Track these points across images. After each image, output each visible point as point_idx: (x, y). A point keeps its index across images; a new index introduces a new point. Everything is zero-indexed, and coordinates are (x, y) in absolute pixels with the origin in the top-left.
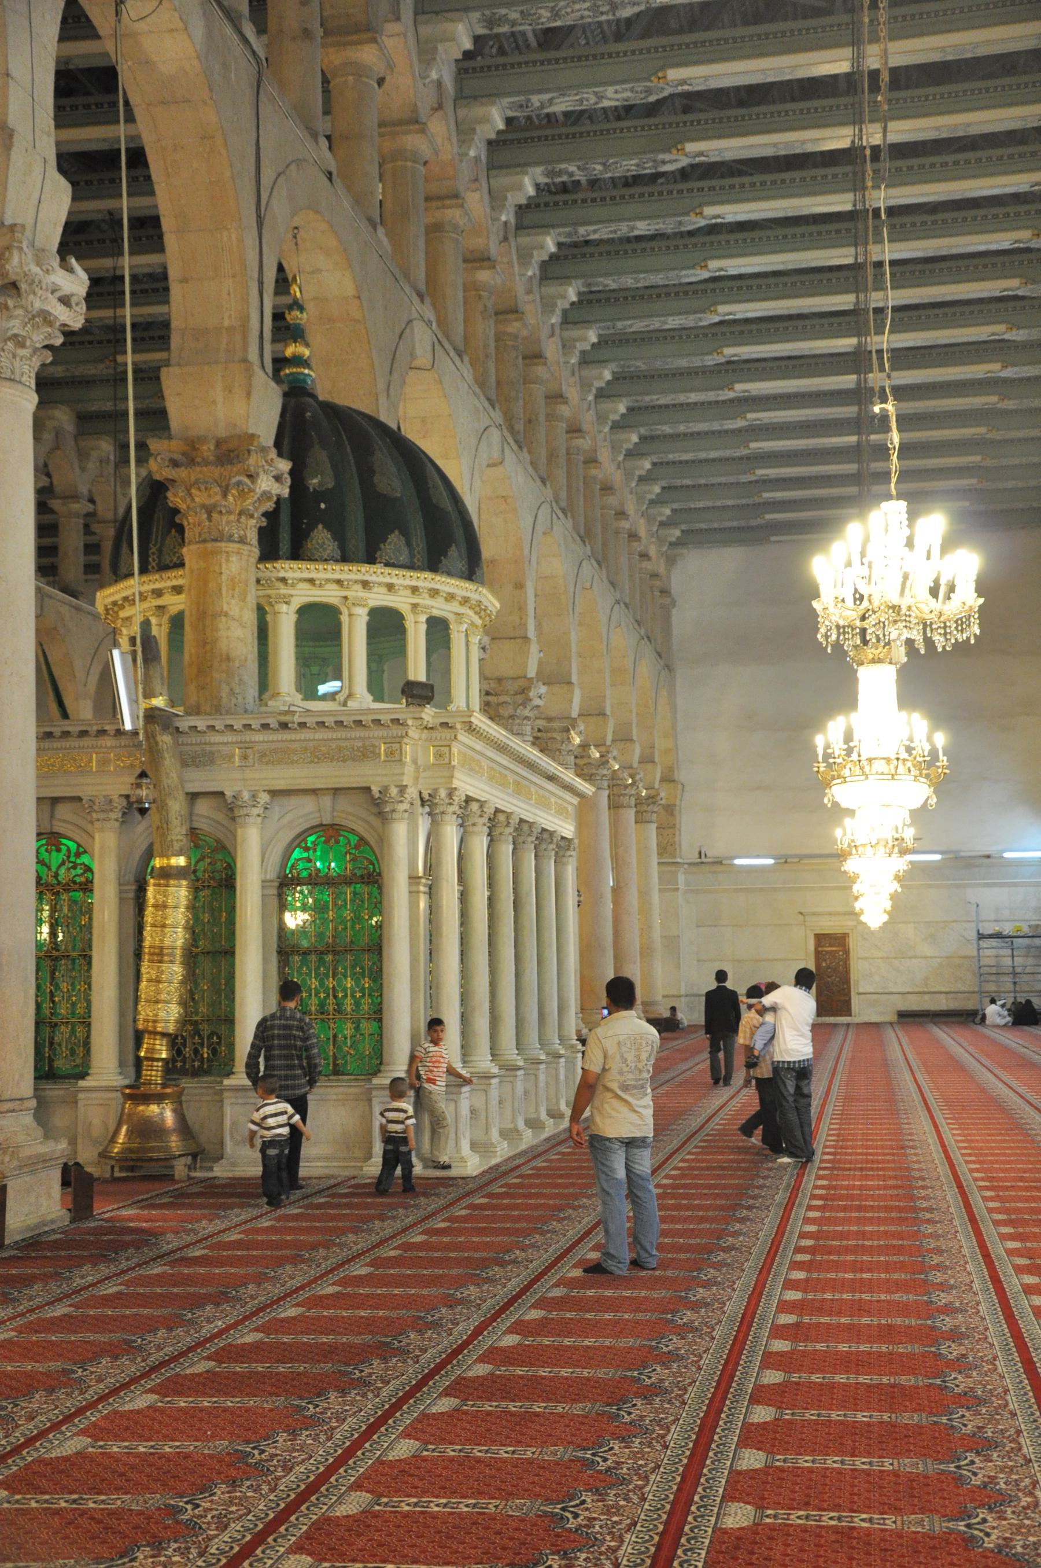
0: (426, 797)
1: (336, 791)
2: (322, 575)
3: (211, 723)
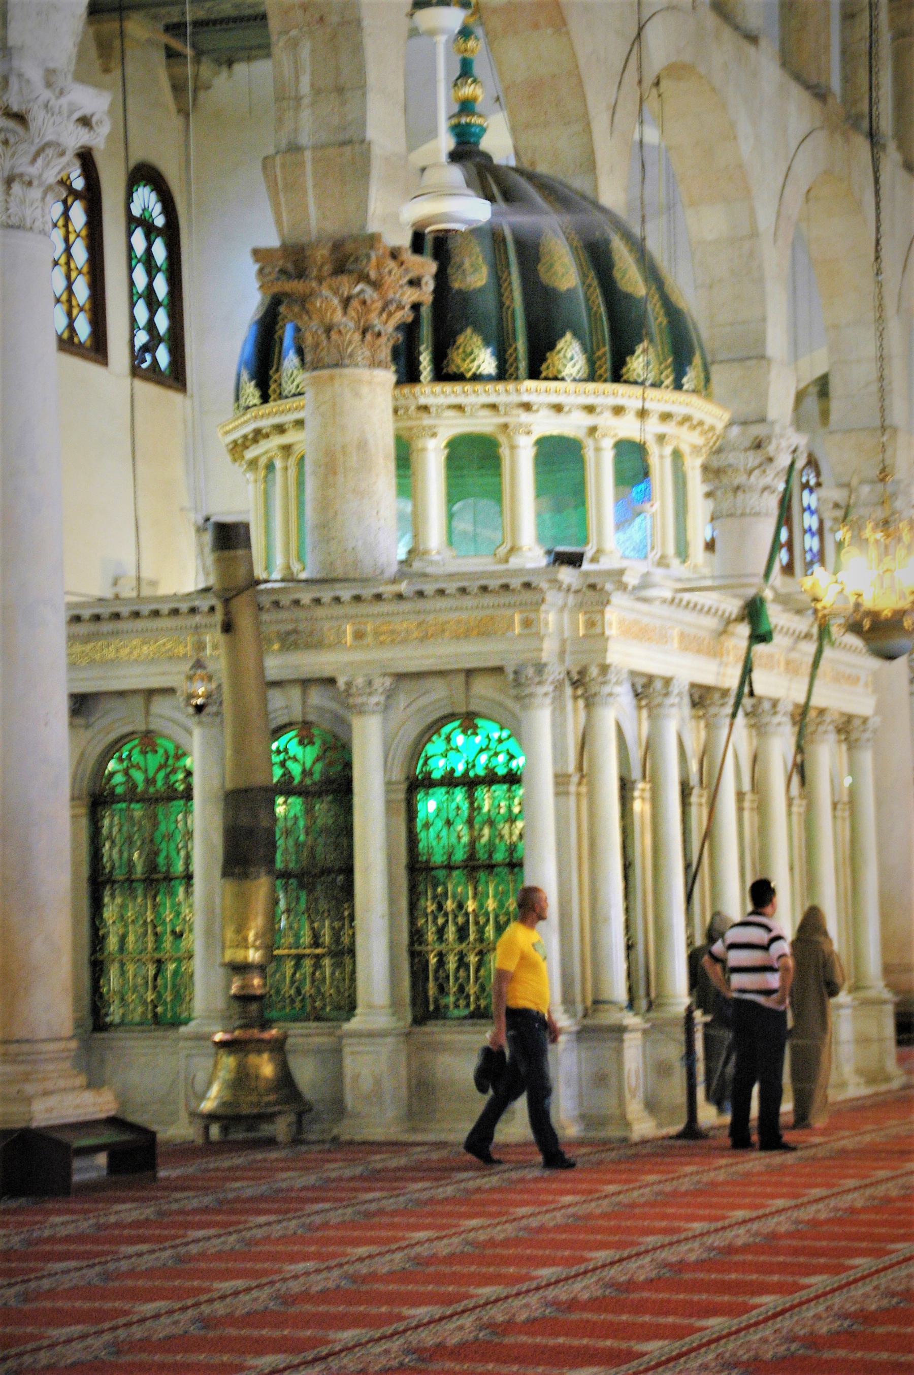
3: (317, 595)
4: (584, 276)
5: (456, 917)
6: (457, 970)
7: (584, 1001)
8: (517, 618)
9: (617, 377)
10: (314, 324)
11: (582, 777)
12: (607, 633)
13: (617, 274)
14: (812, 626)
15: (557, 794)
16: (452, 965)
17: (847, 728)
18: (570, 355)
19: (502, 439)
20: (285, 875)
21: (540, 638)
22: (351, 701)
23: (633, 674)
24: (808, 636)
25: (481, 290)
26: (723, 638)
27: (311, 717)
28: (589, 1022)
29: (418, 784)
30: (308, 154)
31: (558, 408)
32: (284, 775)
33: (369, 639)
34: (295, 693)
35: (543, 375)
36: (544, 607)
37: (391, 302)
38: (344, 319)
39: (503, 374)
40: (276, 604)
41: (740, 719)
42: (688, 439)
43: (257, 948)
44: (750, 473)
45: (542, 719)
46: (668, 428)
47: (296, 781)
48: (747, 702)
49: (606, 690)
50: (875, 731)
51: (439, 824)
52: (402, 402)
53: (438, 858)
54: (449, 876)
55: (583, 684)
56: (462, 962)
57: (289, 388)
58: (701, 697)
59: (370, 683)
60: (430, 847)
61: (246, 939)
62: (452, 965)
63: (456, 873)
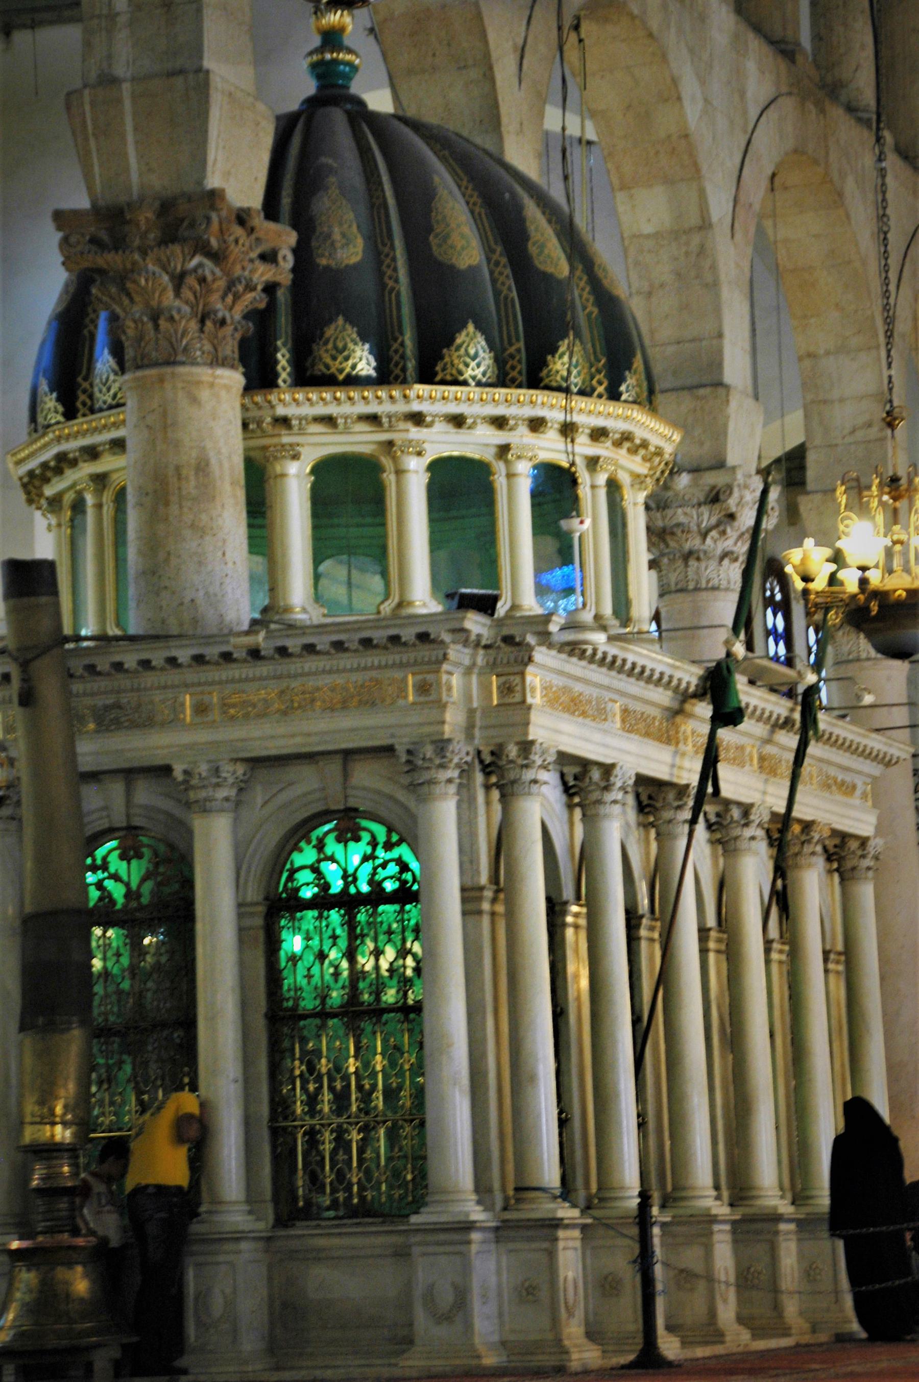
1: (348, 755)
3: (145, 656)
4: (489, 251)
5: (331, 1080)
6: (334, 1153)
7: (504, 1189)
8: (410, 680)
9: (535, 379)
10: (137, 310)
11: (497, 891)
12: (529, 700)
13: (533, 249)
14: (792, 710)
15: (465, 913)
16: (327, 1147)
17: (842, 853)
18: (474, 354)
19: (386, 462)
20: (102, 1033)
21: (443, 707)
22: (192, 795)
23: (564, 758)
24: (787, 723)
25: (356, 267)
26: (679, 719)
27: (137, 821)
28: (508, 1215)
29: (281, 906)
30: (126, 87)
31: (458, 421)
32: (101, 899)
33: (215, 715)
34: (117, 788)
35: (438, 378)
36: (445, 667)
37: (239, 280)
38: (177, 303)
39: (386, 375)
40: (91, 669)
41: (700, 827)
42: (628, 465)
43: (65, 1124)
44: (704, 536)
45: (445, 814)
46: (602, 450)
47: (119, 906)
48: (710, 809)
49: (529, 775)
50: (876, 858)
51: (310, 958)
52: (254, 413)
53: (309, 1003)
54: (323, 1027)
55: (499, 769)
56: (341, 1143)
57: (103, 397)
58: (651, 795)
59: (217, 771)
60: (298, 989)
61: (52, 1113)
62: (327, 1147)
63: (331, 1022)
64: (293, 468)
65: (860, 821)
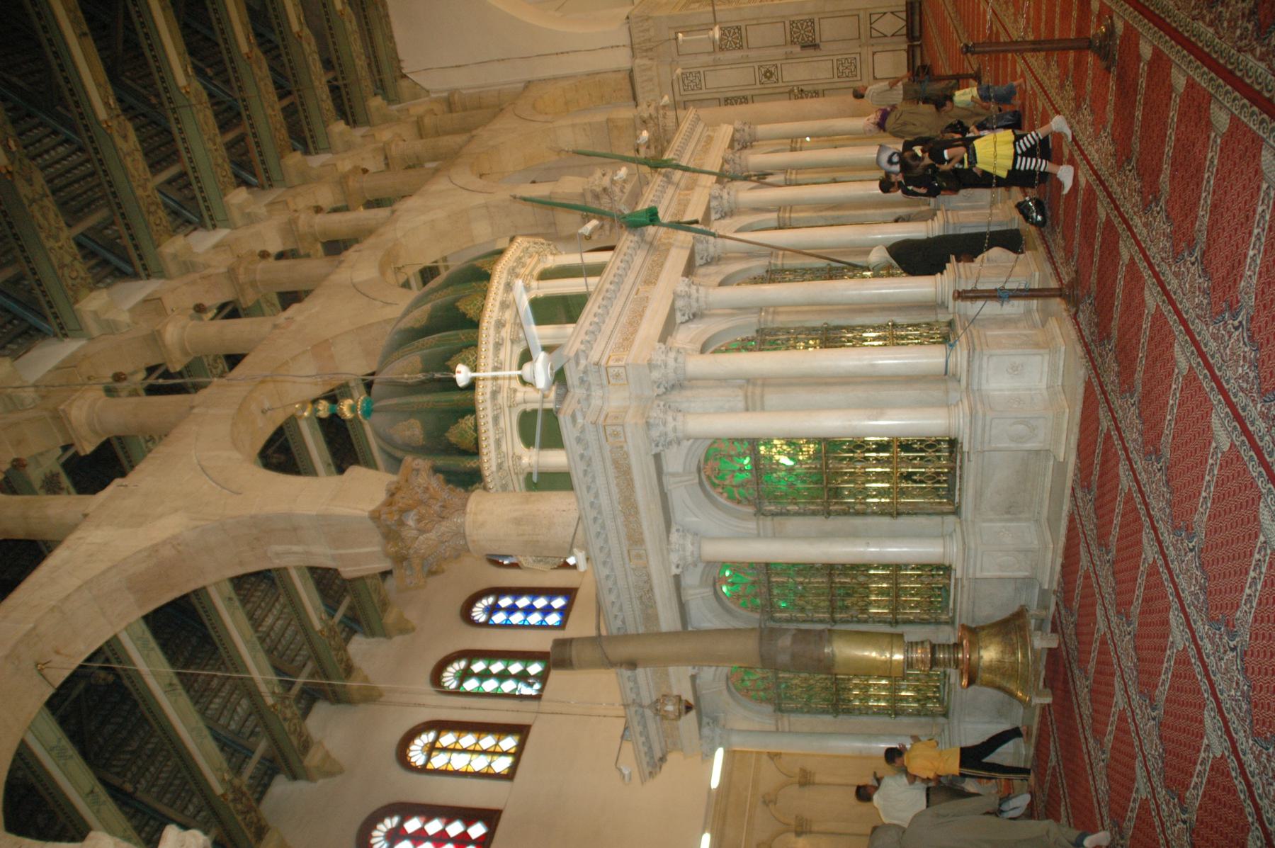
0: (662, 390)
2: (491, 434)
13: (417, 326)
17: (741, 143)
64: (525, 460)
65: (726, 132)
